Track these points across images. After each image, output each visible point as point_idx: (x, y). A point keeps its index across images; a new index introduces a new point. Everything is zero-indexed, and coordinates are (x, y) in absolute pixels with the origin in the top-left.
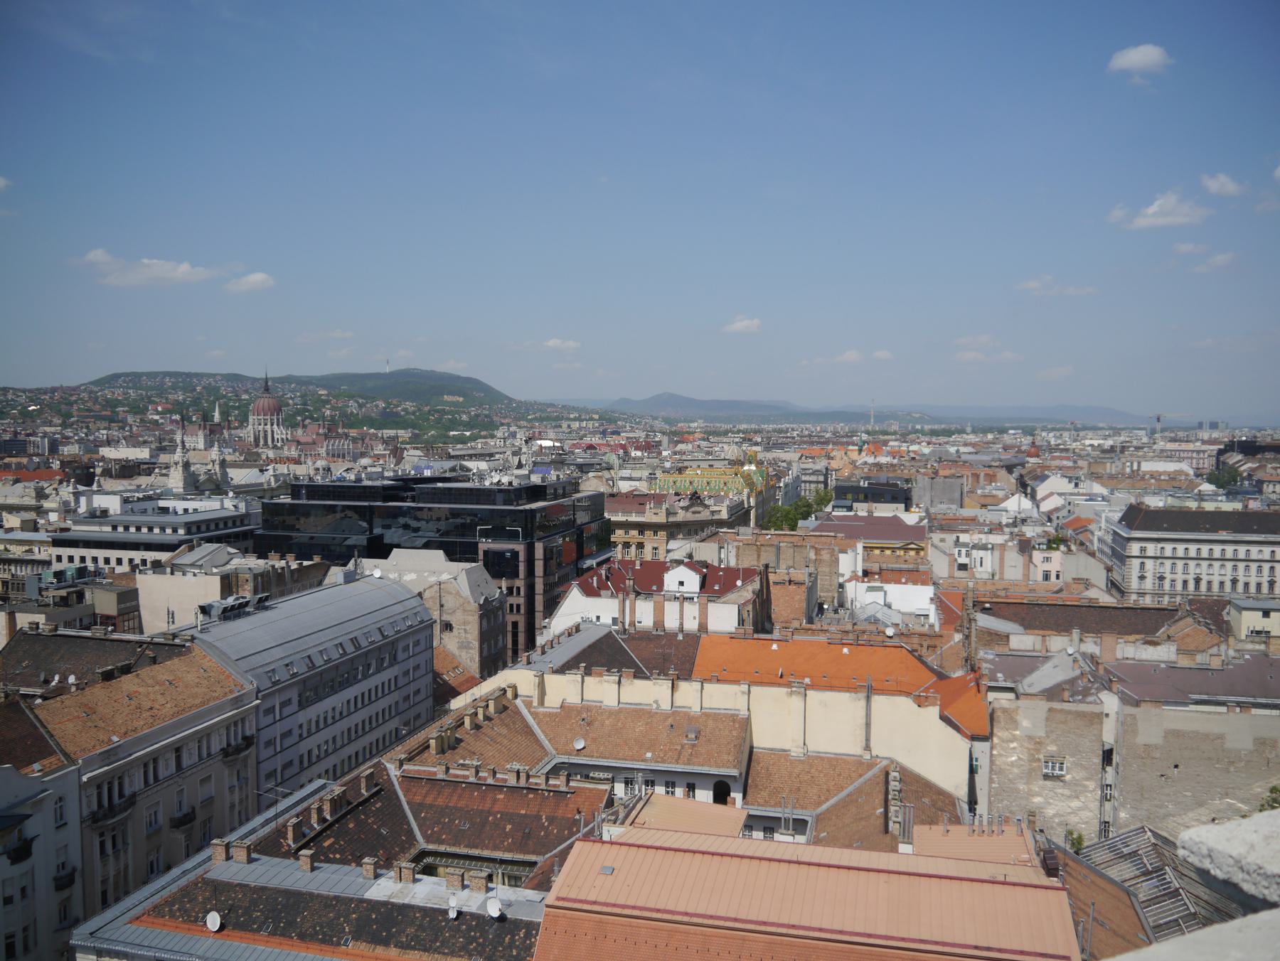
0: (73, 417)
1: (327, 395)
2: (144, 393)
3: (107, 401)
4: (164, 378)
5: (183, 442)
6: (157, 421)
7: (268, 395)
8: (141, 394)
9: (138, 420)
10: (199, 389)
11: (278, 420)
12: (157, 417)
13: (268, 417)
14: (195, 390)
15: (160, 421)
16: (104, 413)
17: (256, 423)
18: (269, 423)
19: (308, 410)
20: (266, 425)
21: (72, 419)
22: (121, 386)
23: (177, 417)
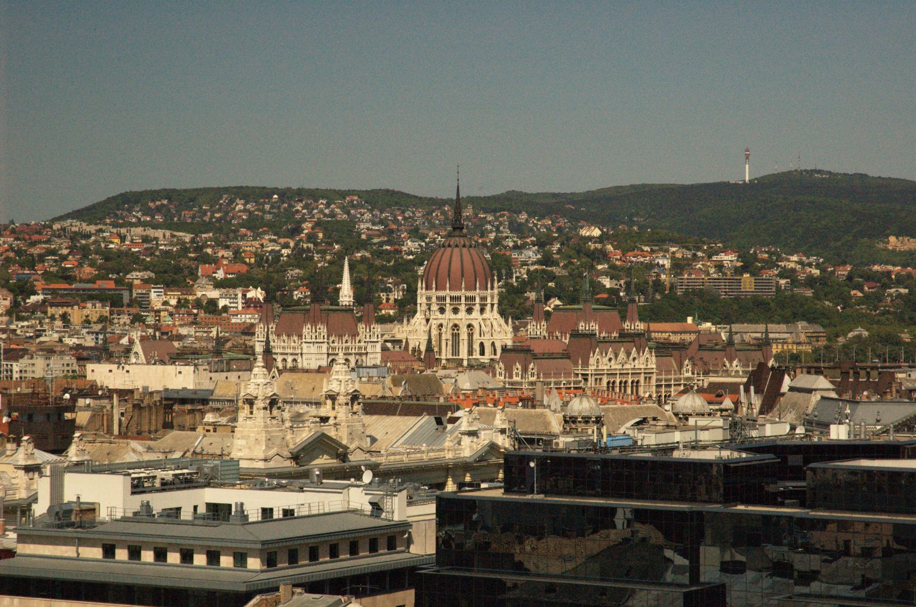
0: (35, 293)
1: (600, 239)
2: (187, 237)
3: (108, 255)
4: (232, 201)
5: (268, 351)
6: (213, 303)
7: (461, 241)
8: (182, 243)
9: (173, 302)
10: (307, 226)
11: (484, 299)
12: (214, 294)
13: (462, 293)
14: (297, 230)
15: (222, 303)
16: (101, 284)
17: (435, 307)
18: (463, 308)
19: (552, 277)
20: (456, 311)
21: (33, 299)
22: (139, 223)
23: (257, 294)
